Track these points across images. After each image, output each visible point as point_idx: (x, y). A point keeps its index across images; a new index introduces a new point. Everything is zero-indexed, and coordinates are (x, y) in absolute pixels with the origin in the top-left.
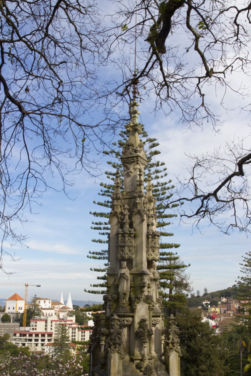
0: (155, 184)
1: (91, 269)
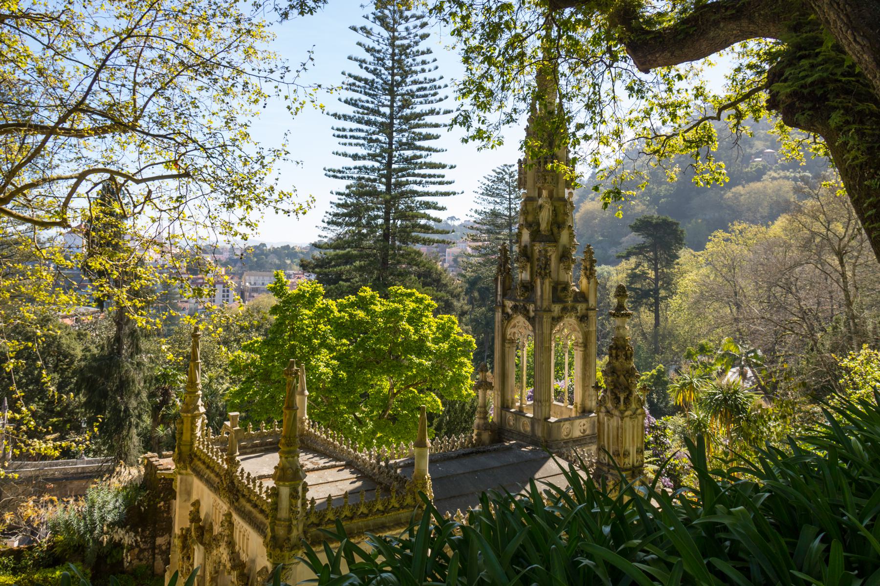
0: (422, 79)
1: (332, 193)
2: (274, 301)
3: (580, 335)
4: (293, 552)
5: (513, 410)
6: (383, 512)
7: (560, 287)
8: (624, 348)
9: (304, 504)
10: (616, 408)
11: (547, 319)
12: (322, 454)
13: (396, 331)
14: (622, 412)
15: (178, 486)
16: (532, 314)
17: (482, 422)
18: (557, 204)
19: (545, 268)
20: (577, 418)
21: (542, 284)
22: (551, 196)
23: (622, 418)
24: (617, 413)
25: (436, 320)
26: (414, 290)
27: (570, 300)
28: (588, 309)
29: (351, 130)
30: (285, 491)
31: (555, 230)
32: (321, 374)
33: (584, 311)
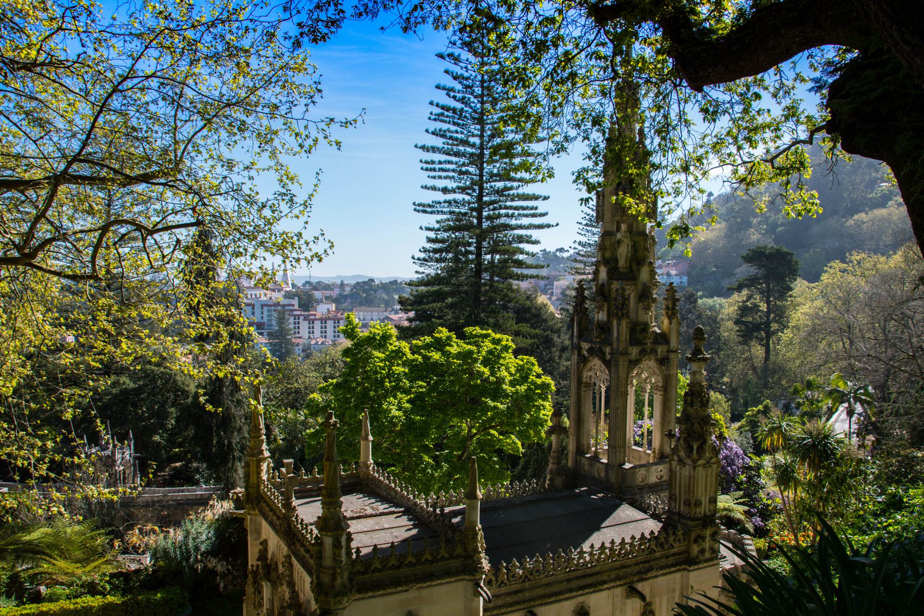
1: (421, 228)
2: (348, 343)
3: (660, 378)
4: (338, 599)
5: (588, 455)
6: (432, 562)
7: (638, 329)
8: (700, 395)
9: (349, 553)
10: (689, 457)
11: (623, 362)
12: (383, 499)
13: (473, 375)
14: (695, 461)
15: (248, 524)
16: (608, 357)
17: (555, 467)
19: (622, 308)
20: (654, 464)
21: (619, 325)
23: (694, 468)
24: (689, 462)
25: (517, 361)
26: (490, 331)
27: (649, 342)
28: (670, 351)
29: (440, 163)
30: (328, 541)
31: (635, 267)
32: (394, 417)
33: (665, 353)
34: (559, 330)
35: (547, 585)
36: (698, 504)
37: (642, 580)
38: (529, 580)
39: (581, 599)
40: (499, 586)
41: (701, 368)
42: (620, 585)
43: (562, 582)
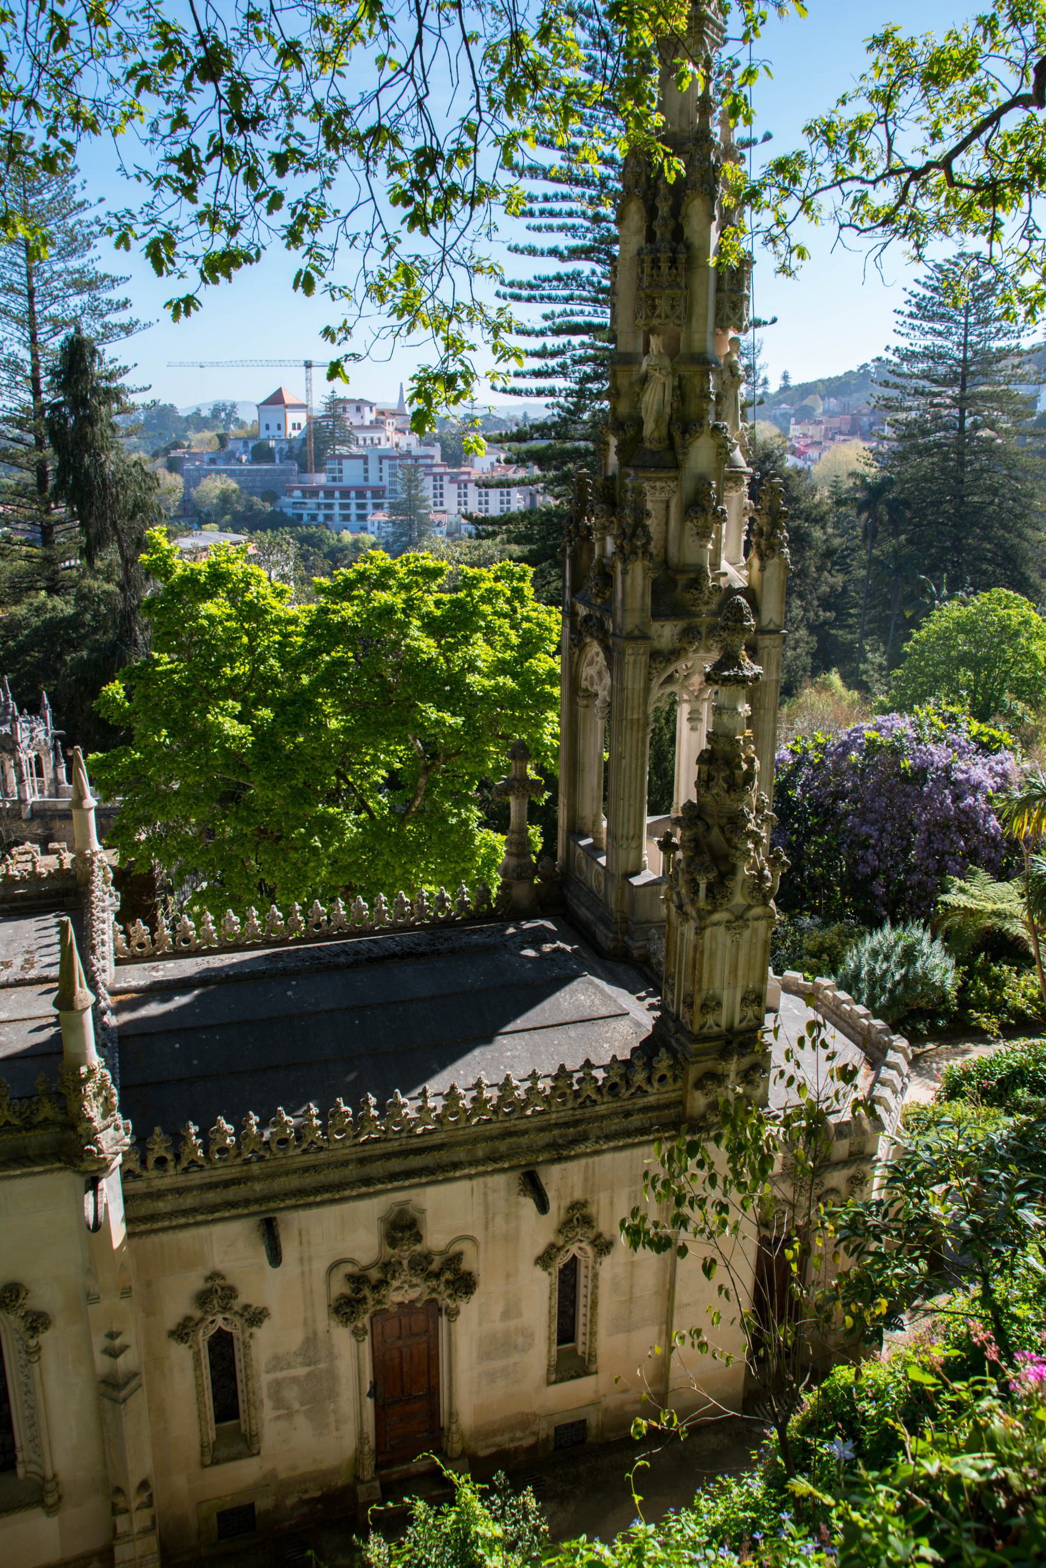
14: (702, 915)
18: (685, 370)
19: (634, 535)
21: (625, 572)
22: (672, 351)
29: (546, 199)
34: (822, 518)
35: (306, 1170)
36: (712, 1004)
37: (560, 1159)
38: (261, 1159)
39: (400, 1196)
40: (186, 1170)
41: (735, 700)
42: (504, 1170)
43: (345, 1164)
